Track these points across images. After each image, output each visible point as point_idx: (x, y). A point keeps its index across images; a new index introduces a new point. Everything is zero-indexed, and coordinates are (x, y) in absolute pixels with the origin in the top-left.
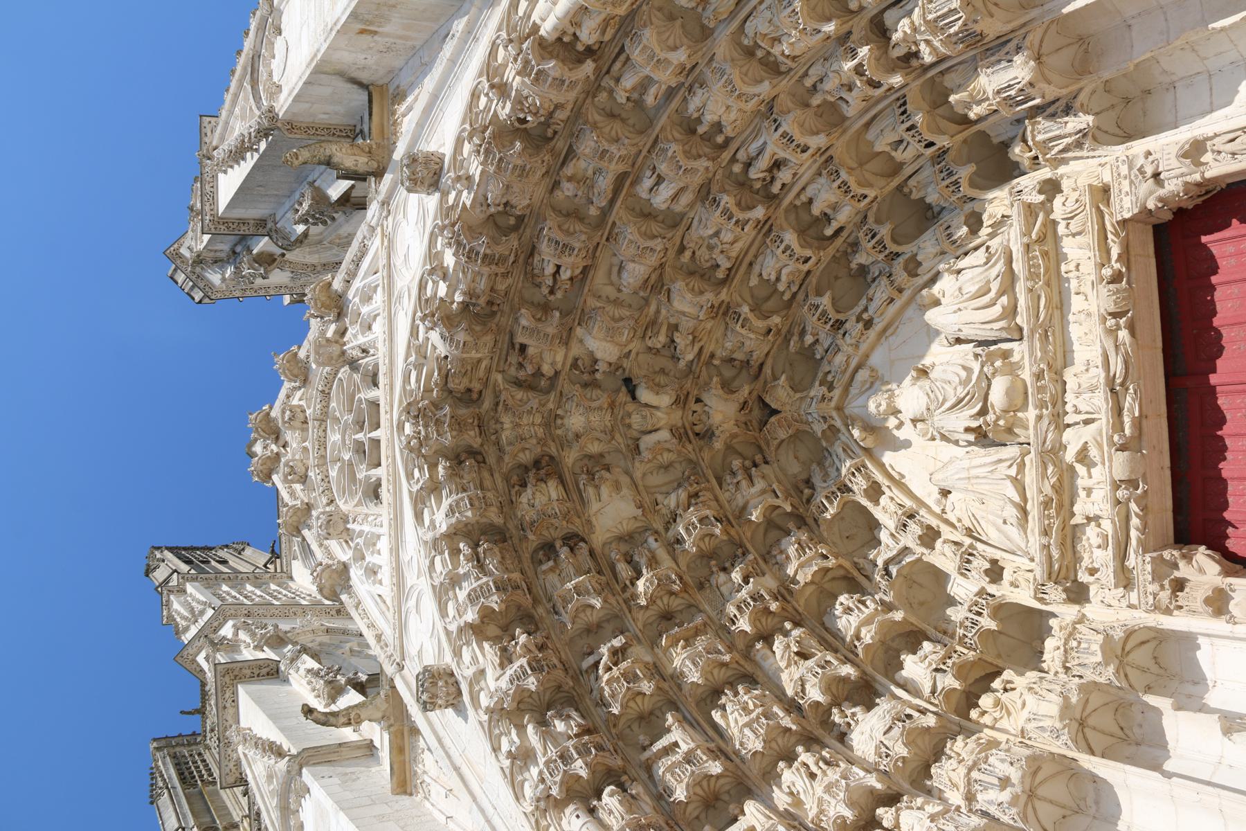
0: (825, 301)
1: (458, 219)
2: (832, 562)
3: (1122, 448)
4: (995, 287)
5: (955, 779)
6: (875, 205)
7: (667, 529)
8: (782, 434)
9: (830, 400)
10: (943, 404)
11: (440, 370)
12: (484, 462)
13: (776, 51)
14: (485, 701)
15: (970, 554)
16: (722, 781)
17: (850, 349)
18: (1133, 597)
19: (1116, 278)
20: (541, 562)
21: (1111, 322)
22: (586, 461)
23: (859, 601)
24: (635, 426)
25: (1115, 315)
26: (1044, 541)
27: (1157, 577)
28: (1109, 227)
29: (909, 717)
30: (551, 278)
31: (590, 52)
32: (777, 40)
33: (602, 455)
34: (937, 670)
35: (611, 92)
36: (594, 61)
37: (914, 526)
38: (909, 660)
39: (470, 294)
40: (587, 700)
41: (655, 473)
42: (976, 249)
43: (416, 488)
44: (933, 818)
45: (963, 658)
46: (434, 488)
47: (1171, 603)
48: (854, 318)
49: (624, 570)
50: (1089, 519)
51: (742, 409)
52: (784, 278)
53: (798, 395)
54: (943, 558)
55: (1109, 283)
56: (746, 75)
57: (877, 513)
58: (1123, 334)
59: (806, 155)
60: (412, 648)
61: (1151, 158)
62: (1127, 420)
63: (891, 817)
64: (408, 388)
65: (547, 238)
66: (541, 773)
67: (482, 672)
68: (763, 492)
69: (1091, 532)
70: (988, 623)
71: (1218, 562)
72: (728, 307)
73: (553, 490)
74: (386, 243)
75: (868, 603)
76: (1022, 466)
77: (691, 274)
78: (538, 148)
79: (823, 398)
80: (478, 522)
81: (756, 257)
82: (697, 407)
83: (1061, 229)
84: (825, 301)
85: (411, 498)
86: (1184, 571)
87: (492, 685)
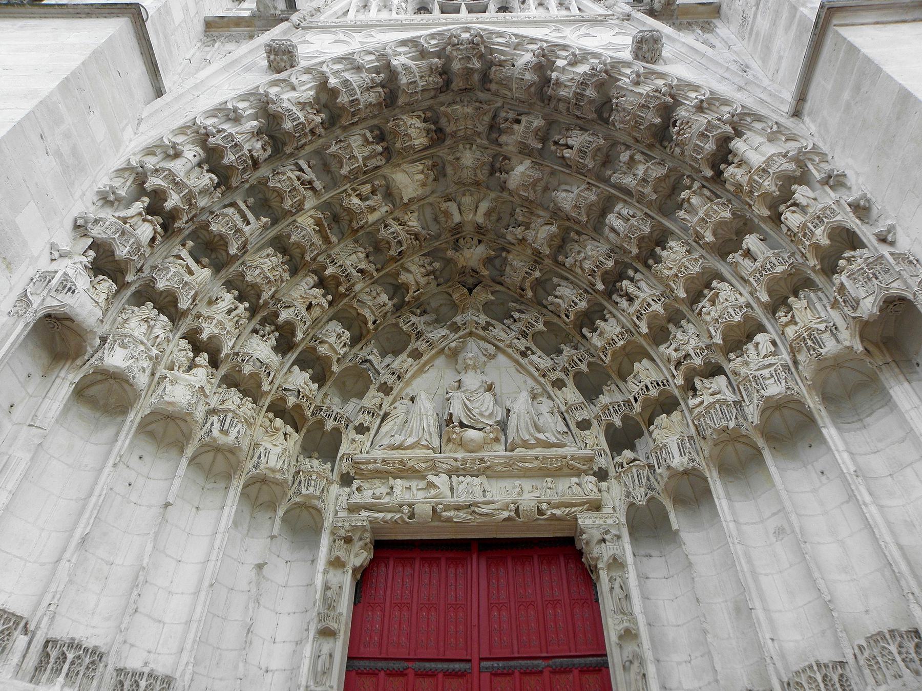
0: (540, 326)
1: (610, 76)
2: (370, 326)
4: (541, 436)
5: (226, 403)
6: (601, 363)
7: (394, 219)
8: (455, 296)
9: (476, 328)
10: (468, 400)
11: (505, 61)
12: (441, 92)
13: (705, 302)
14: (273, 91)
15: (373, 414)
16: (224, 254)
17: (509, 342)
19: (540, 512)
20: (372, 132)
21: (513, 507)
22: (441, 165)
23: (345, 344)
24: (463, 199)
25: (517, 509)
26: (379, 461)
27: (355, 528)
28: (573, 510)
29: (269, 374)
30: (564, 142)
31: (719, 174)
32: (713, 304)
33: (445, 175)
34: (299, 392)
35: (690, 188)
36: (712, 177)
37: (393, 379)
38: (306, 375)
39: (558, 83)
40: (277, 163)
41: (432, 211)
42: (567, 425)
43: (422, 41)
44: (202, 388)
45: (307, 409)
46: (423, 54)
47: (338, 536)
48: (528, 346)
49: (366, 189)
50: (392, 488)
51: (473, 271)
52: (557, 300)
53: (481, 308)
54: (372, 398)
55: (538, 507)
56: (692, 282)
57: (403, 356)
58: (505, 514)
59: (635, 318)
60: (310, 36)
61: (615, 538)
63: (201, 362)
64: (494, 36)
65: (592, 140)
66: (224, 130)
67: (294, 89)
68: (417, 283)
69: (384, 490)
70: (330, 424)
71: (361, 566)
72: (539, 263)
73: (420, 141)
74: (600, 18)
75: (345, 349)
76: (427, 447)
77: (563, 240)
78: (654, 135)
79: (477, 323)
80: (399, 87)
81: (572, 283)
82: (475, 241)
84: (540, 326)
85: (416, 37)
86: (358, 545)
87: (285, 96)
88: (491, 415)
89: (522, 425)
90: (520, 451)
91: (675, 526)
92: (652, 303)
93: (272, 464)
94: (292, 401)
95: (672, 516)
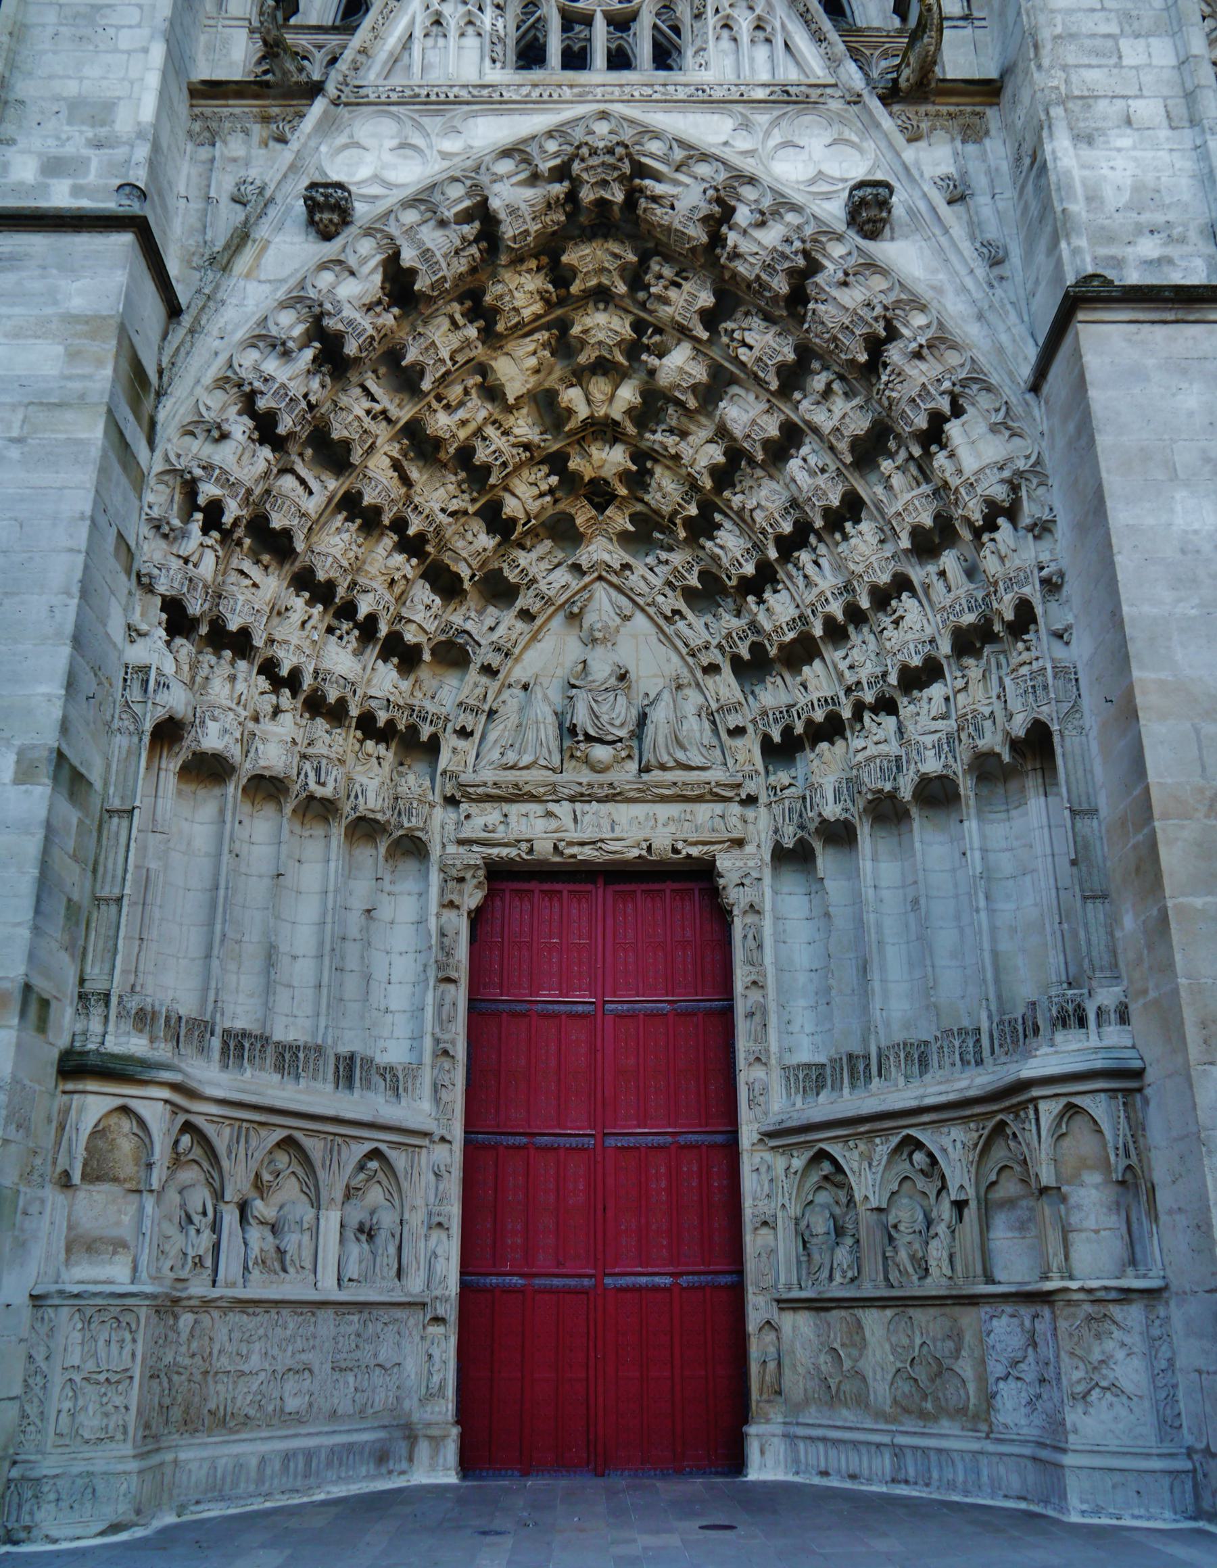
3: (556, 847)
4: (680, 756)
18: (452, 849)
19: (675, 851)
21: (645, 845)
25: (649, 848)
27: (468, 867)
38: (394, 674)
42: (716, 731)
58: (635, 852)
59: (809, 611)
62: (575, 850)
70: (426, 731)
76: (546, 767)
83: (718, 808)
86: (471, 883)
88: (622, 725)
89: (661, 741)
90: (656, 775)
91: (821, 874)
92: (831, 599)
93: (371, 805)
94: (382, 717)
95: (820, 861)
